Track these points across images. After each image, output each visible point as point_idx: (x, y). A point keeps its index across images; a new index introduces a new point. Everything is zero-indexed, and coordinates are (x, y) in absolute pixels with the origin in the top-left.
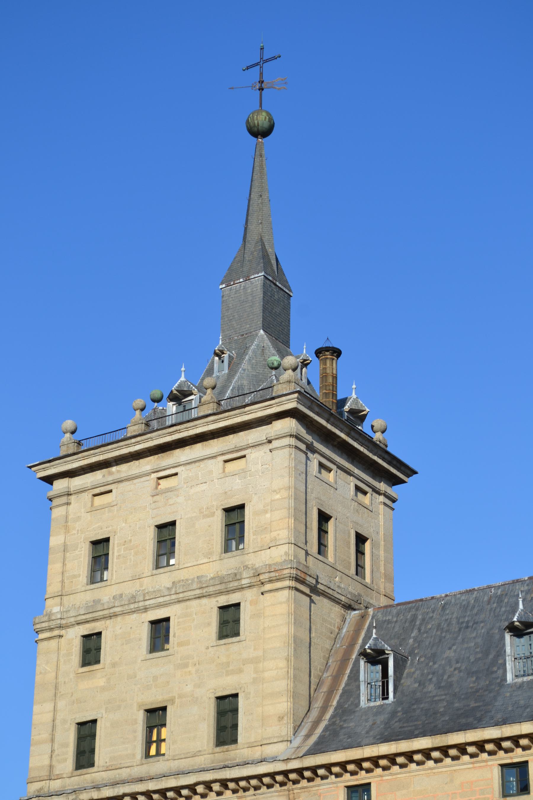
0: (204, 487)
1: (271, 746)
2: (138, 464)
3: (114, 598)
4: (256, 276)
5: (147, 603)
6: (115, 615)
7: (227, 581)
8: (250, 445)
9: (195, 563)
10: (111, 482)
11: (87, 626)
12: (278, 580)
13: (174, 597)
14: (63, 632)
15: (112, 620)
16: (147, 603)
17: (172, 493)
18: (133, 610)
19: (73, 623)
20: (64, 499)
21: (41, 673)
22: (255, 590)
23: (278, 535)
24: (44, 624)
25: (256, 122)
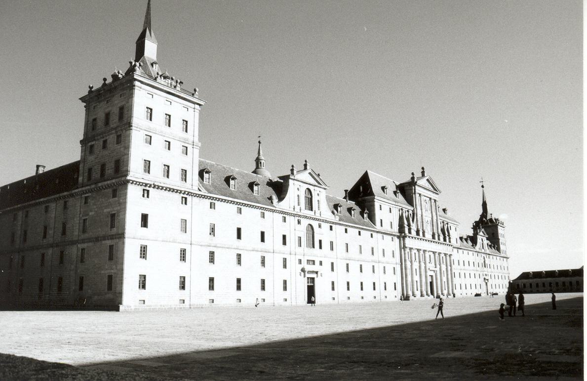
14: (140, 130)
20: (139, 89)
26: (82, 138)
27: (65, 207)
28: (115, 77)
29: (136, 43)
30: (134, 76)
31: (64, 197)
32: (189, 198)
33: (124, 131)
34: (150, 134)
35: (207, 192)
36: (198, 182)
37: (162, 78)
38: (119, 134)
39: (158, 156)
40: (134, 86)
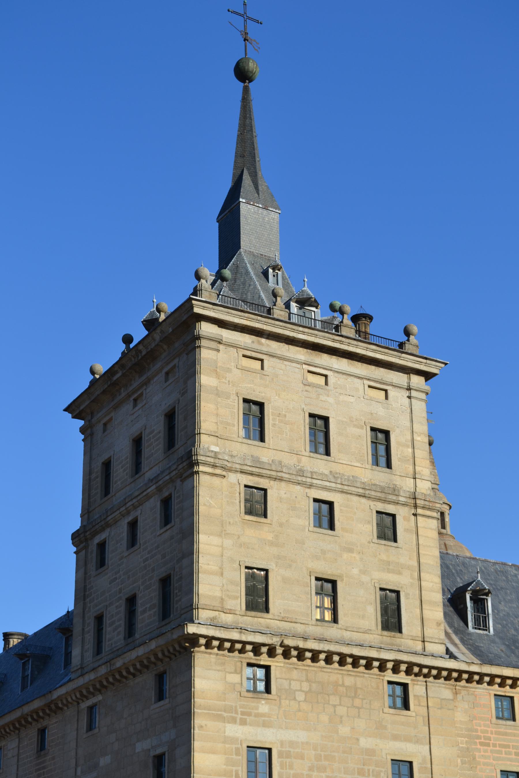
0: (352, 399)
1: (432, 644)
2: (287, 348)
3: (272, 461)
4: (274, 210)
5: (315, 481)
6: (281, 479)
7: (386, 492)
8: (394, 384)
9: (349, 463)
10: (265, 352)
11: (250, 477)
12: (429, 509)
13: (339, 486)
14: (224, 473)
15: (276, 482)
16: (315, 481)
17: (323, 390)
18: (300, 482)
19: (238, 470)
20: (214, 345)
21: (205, 505)
22: (406, 509)
23: (422, 471)
24: (209, 458)
25: (255, 70)
26: (76, 524)
27: (42, 746)
28: (150, 324)
29: (219, 220)
30: (192, 308)
31: (35, 716)
32: (417, 688)
33: (178, 482)
34: (263, 483)
35: (476, 661)
36: (444, 625)
37: (294, 307)
38: (166, 494)
39: (291, 548)
40: (199, 338)
